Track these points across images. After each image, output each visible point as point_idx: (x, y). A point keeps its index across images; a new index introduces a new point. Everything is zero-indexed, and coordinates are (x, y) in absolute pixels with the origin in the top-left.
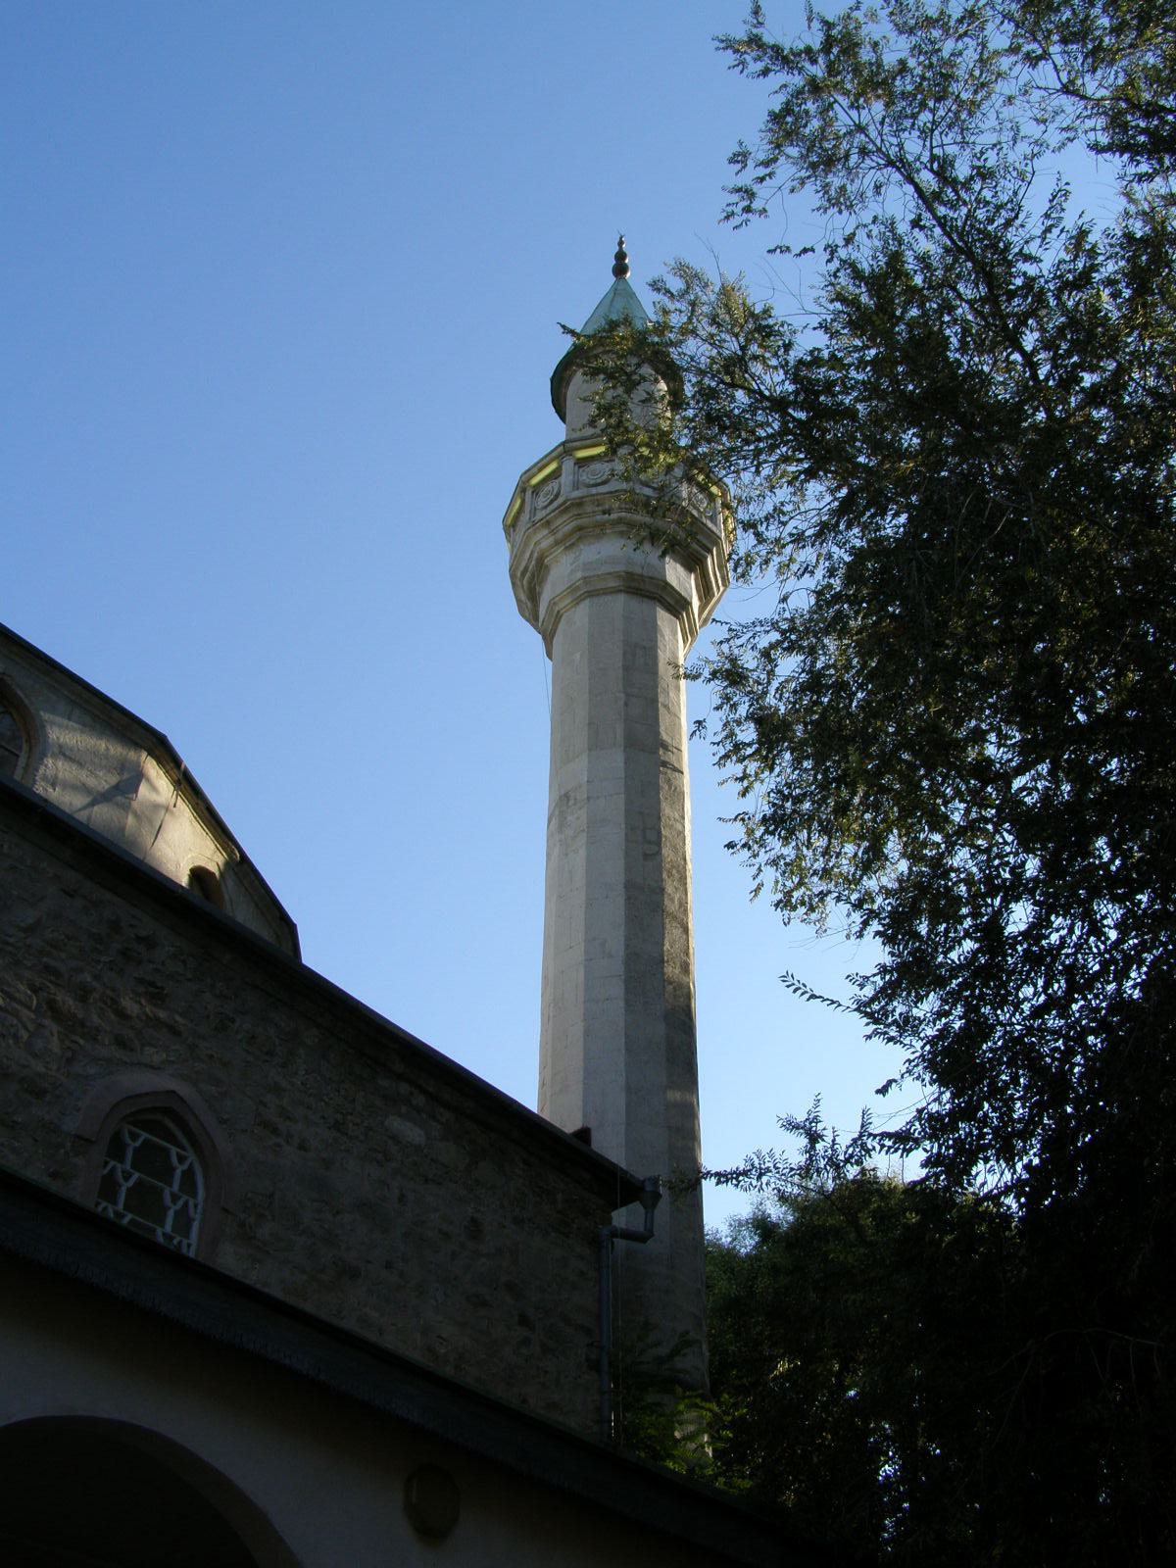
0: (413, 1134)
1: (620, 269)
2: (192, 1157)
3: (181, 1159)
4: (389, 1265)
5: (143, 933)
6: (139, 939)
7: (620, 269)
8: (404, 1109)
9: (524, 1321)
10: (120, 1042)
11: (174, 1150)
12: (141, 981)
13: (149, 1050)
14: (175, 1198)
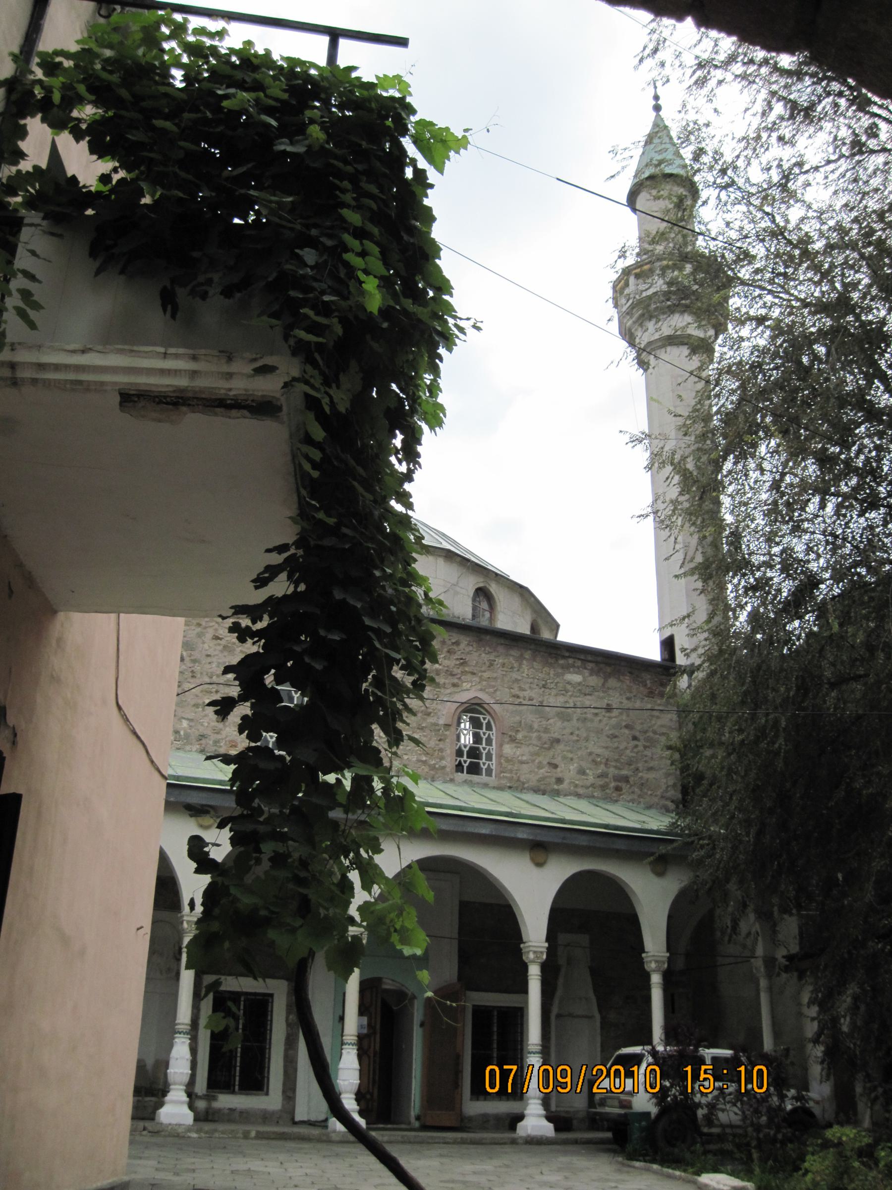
0: (576, 678)
1: (657, 108)
2: (488, 717)
3: (484, 719)
4: (572, 734)
5: (454, 641)
6: (453, 643)
7: (657, 108)
8: (571, 670)
9: (635, 738)
10: (454, 685)
11: (481, 717)
12: (457, 659)
13: (465, 684)
14: (484, 734)
